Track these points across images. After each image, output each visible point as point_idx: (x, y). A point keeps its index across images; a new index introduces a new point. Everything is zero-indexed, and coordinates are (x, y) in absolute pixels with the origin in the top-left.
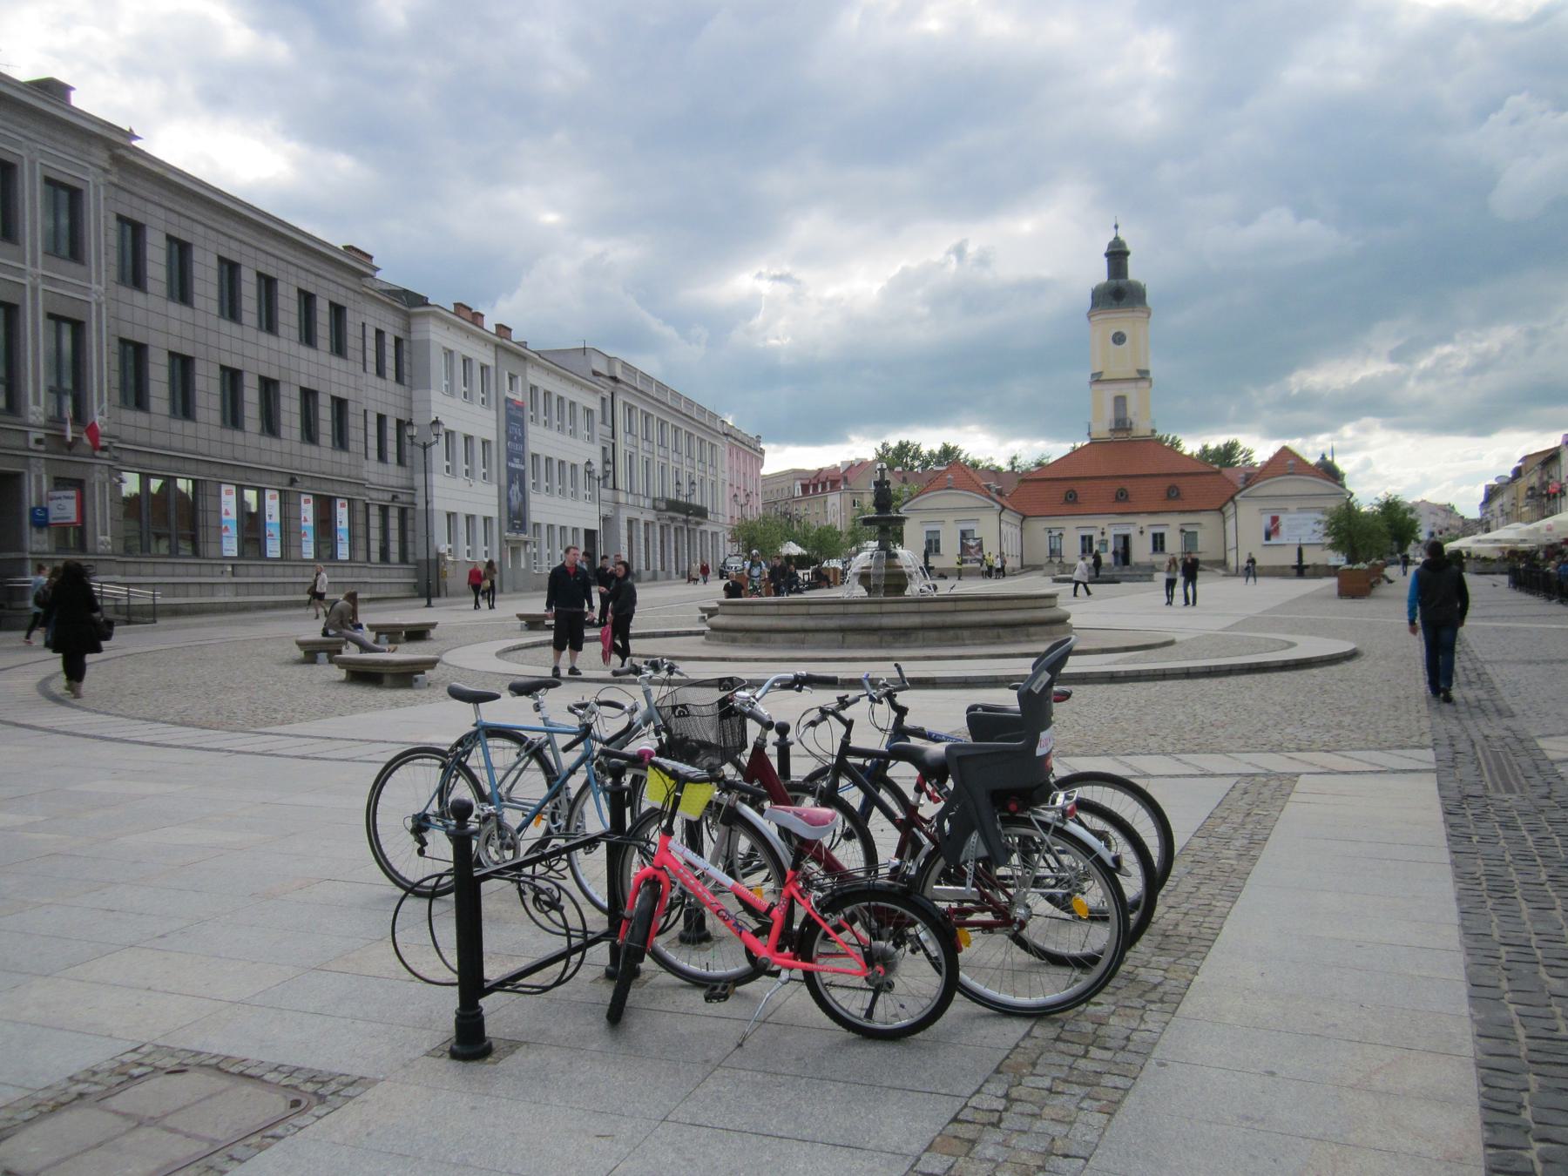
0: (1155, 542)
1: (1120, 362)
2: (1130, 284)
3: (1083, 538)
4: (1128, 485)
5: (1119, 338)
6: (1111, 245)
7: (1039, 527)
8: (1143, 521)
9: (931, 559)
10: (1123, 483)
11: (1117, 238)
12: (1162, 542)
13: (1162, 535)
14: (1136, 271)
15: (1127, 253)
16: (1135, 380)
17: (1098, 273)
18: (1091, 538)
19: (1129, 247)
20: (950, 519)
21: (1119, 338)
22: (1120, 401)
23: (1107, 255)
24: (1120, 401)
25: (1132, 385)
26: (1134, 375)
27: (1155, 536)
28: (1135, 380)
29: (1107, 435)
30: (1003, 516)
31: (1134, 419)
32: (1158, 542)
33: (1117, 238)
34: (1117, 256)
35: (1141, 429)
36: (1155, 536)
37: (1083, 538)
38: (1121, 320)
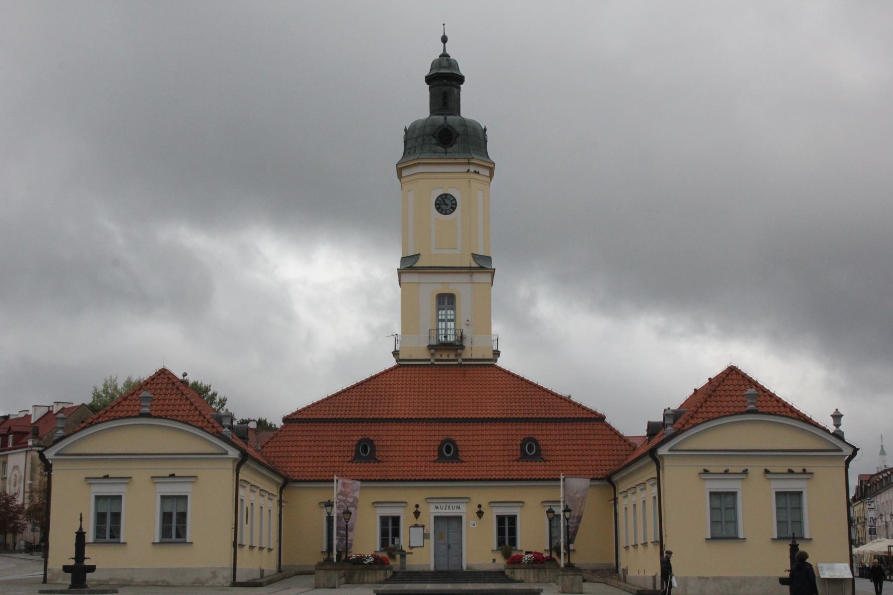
0: (501, 532)
1: (448, 242)
2: (465, 123)
3: (384, 520)
4: (460, 435)
5: (446, 204)
6: (435, 65)
7: (309, 503)
8: (482, 496)
9: (88, 552)
10: (449, 431)
11: (445, 55)
12: (513, 531)
13: (513, 519)
14: (472, 105)
15: (461, 79)
16: (469, 270)
17: (418, 106)
18: (396, 520)
19: (463, 71)
20: (141, 474)
21: (446, 204)
22: (446, 300)
23: (429, 80)
24: (446, 300)
25: (465, 278)
26: (468, 262)
27: (501, 519)
28: (469, 270)
29: (426, 355)
30: (244, 474)
31: (467, 333)
32: (507, 528)
33: (445, 55)
34: (445, 81)
35: (475, 350)
36: (501, 519)
37: (384, 520)
38: (447, 178)
